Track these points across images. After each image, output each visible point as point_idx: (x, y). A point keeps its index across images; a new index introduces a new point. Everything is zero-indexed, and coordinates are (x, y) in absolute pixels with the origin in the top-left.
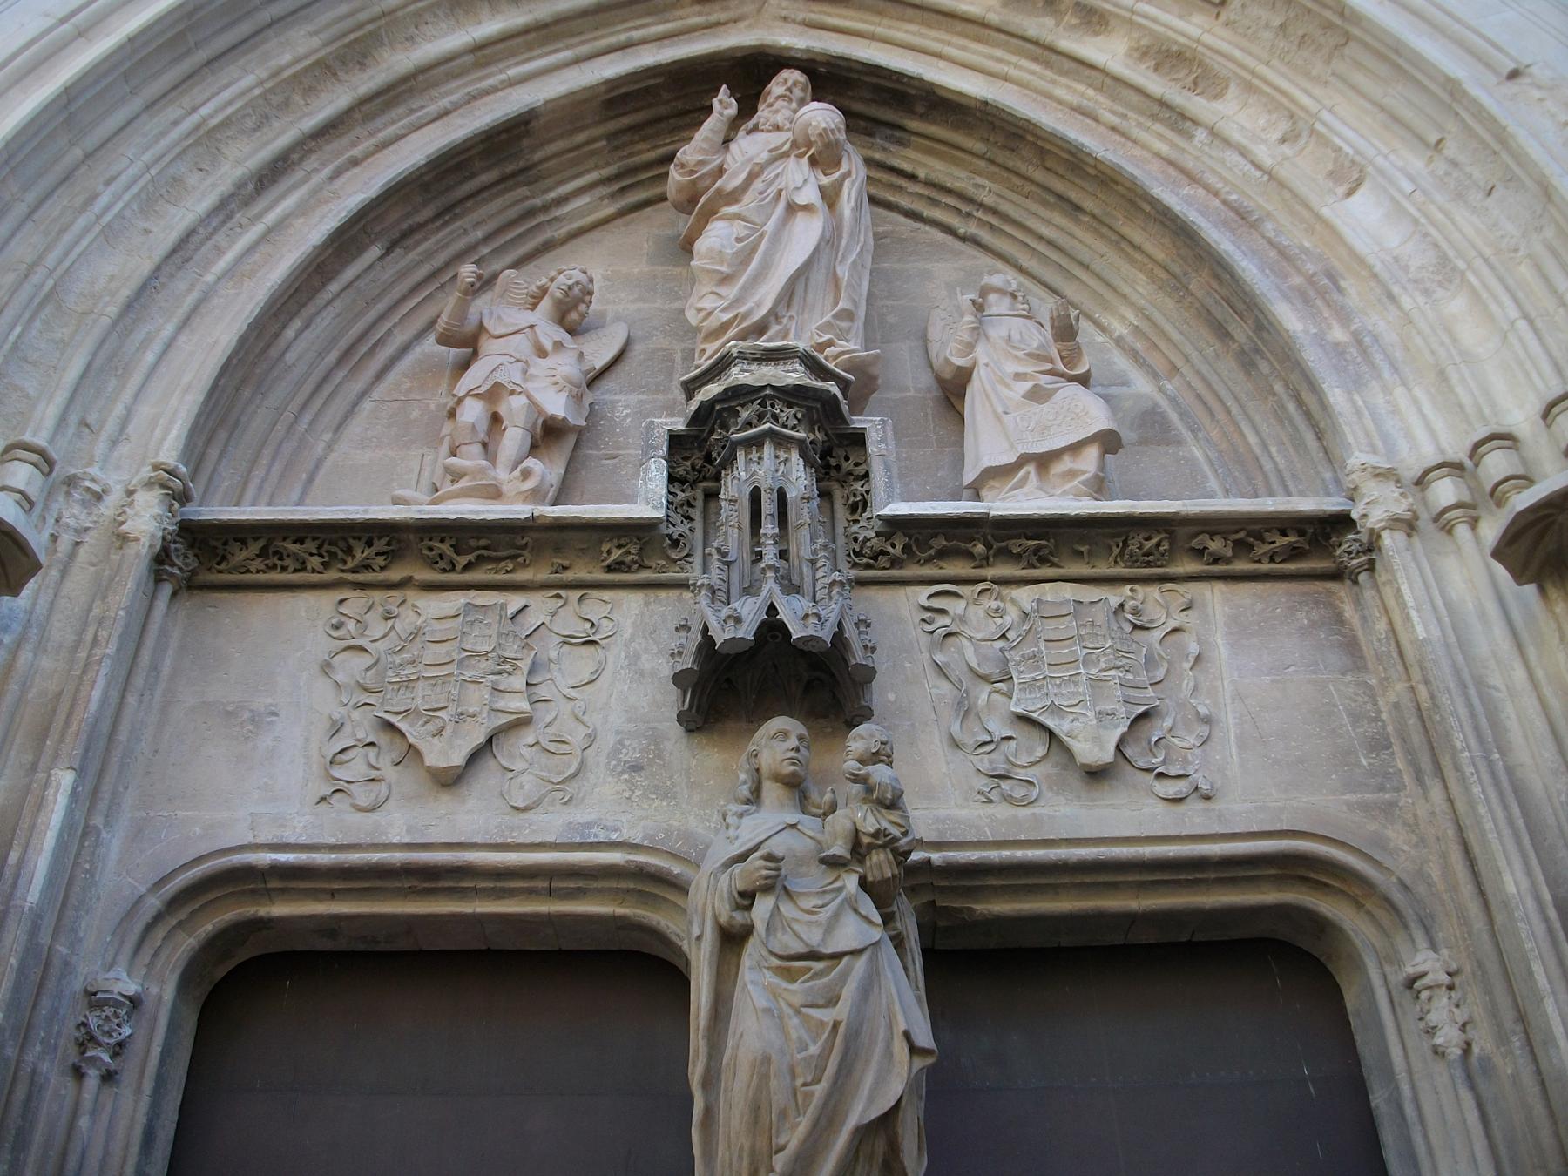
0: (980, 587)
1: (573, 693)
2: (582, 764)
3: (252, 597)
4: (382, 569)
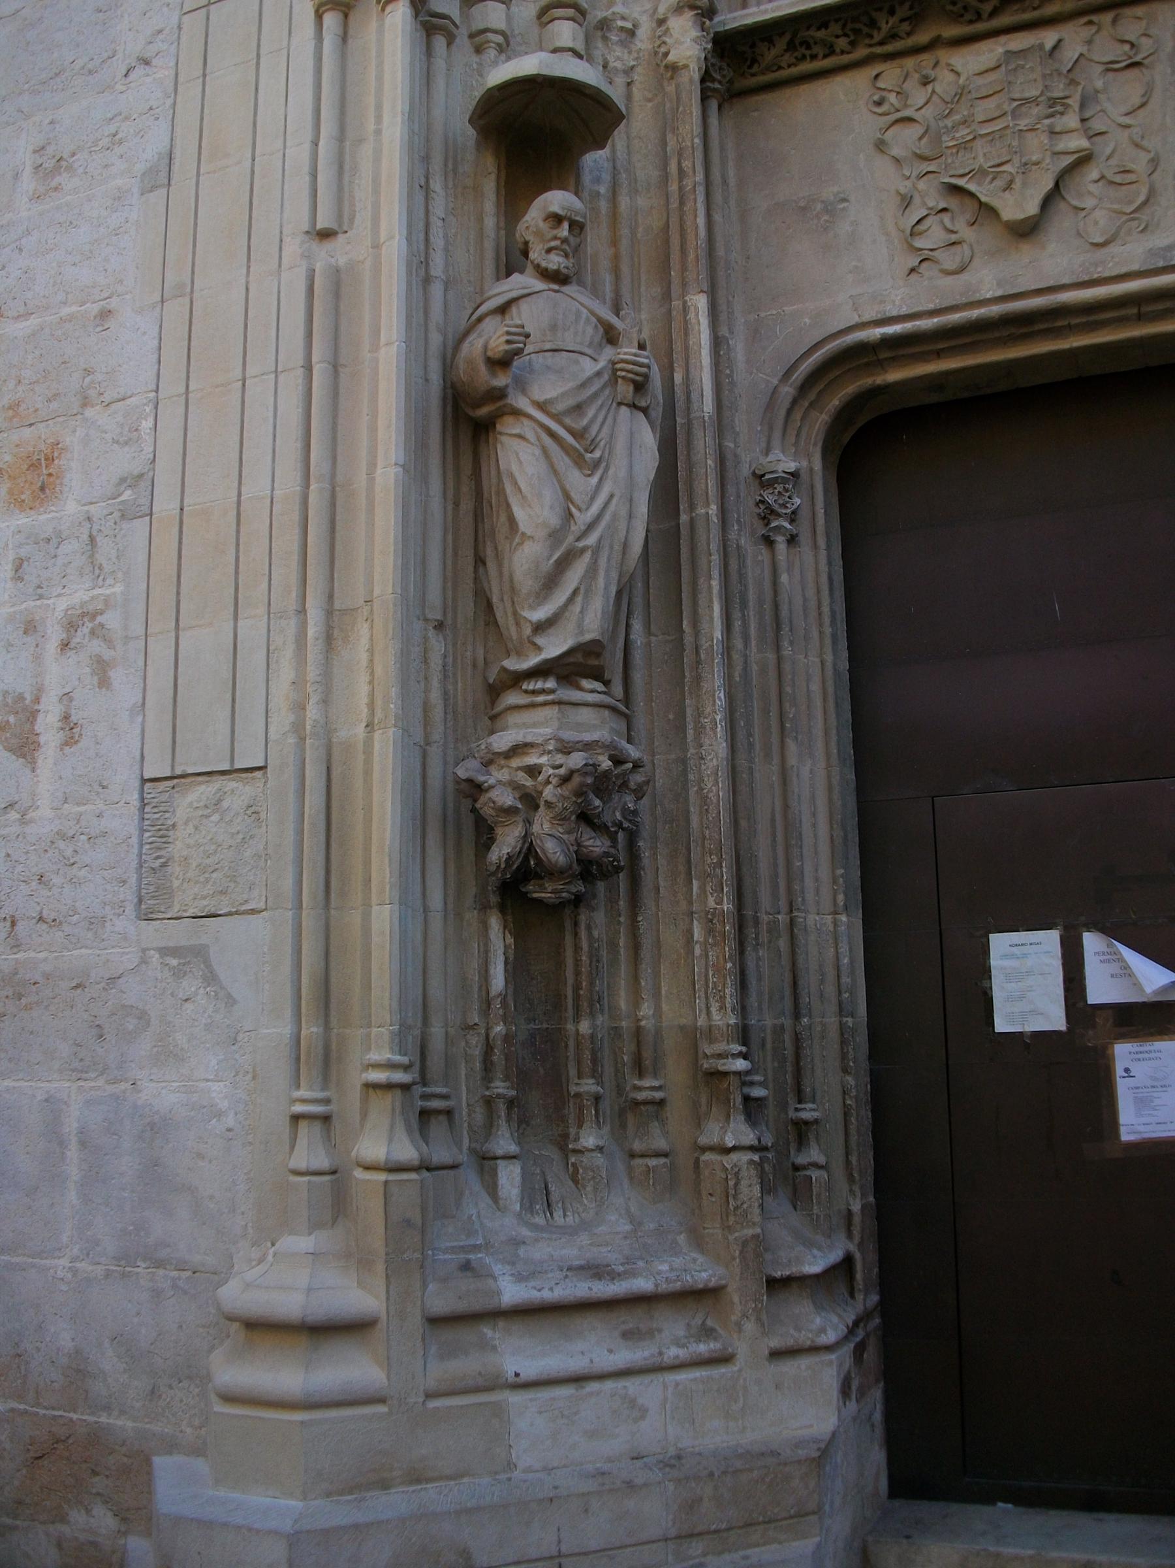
1: (1127, 120)
2: (1152, 193)
3: (788, 92)
4: (909, 34)
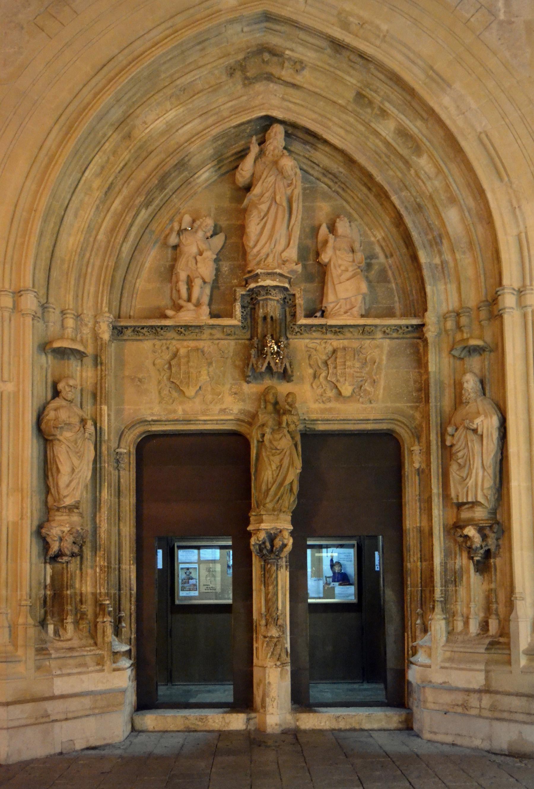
0: (325, 341)
